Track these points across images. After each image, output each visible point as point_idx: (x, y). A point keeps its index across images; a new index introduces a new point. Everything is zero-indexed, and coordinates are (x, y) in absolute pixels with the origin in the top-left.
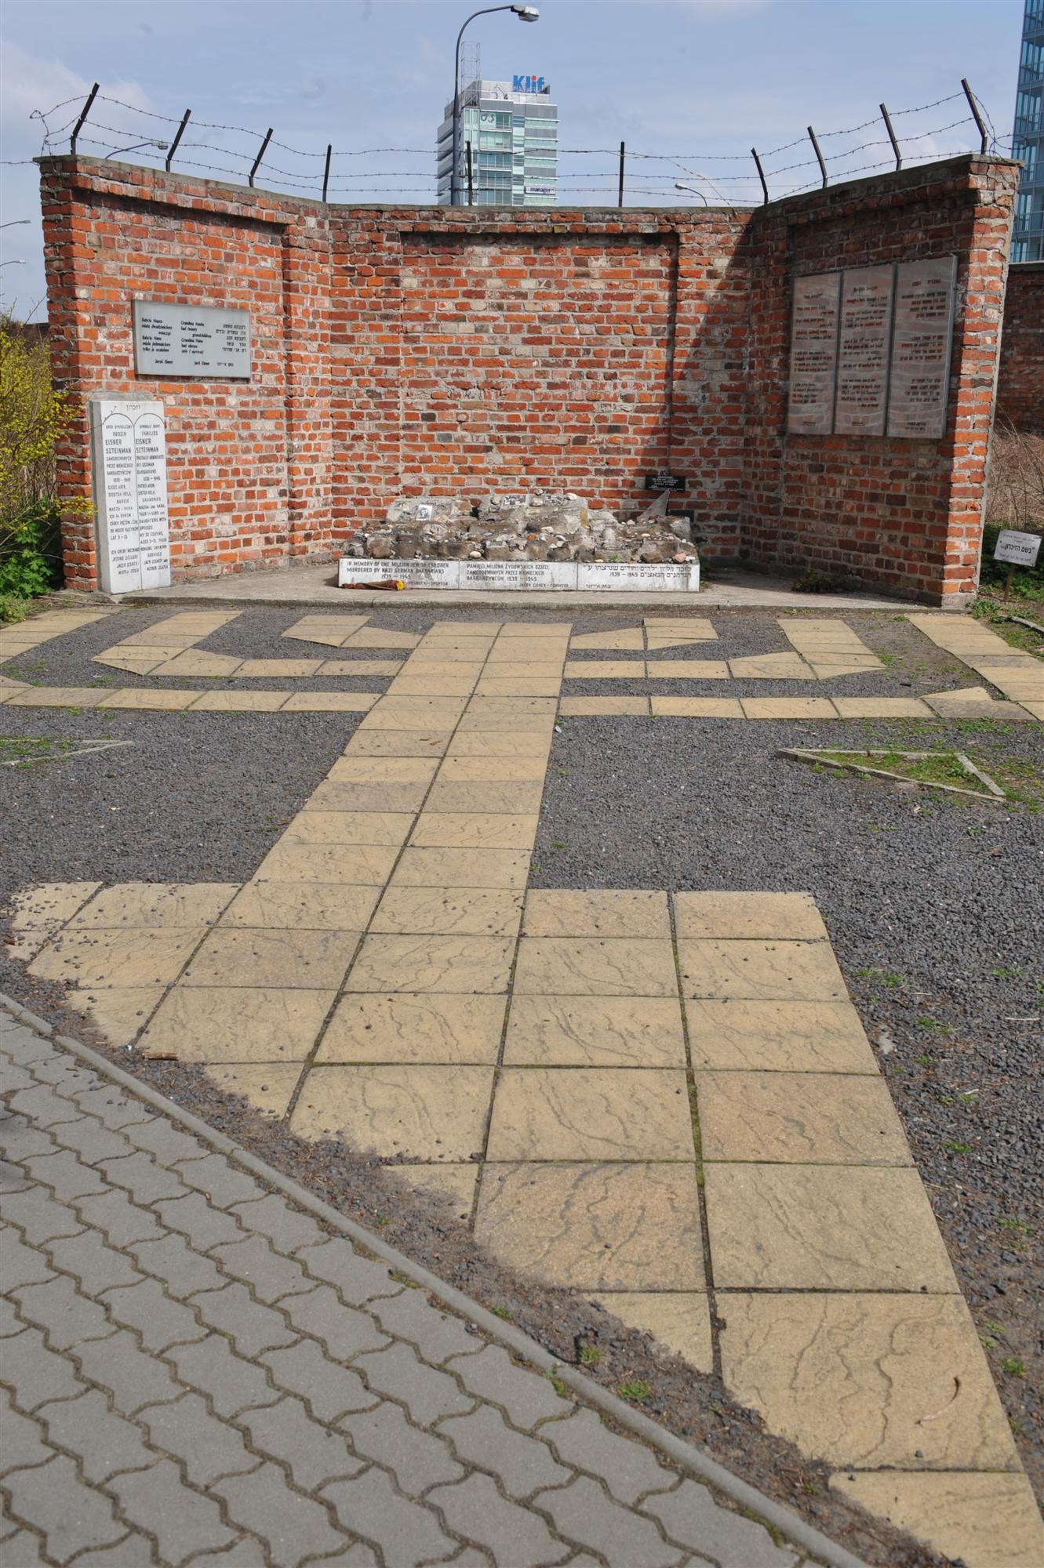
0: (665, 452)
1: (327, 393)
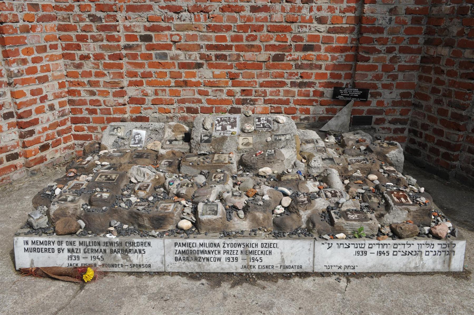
0: (350, 67)
1: (53, 18)
